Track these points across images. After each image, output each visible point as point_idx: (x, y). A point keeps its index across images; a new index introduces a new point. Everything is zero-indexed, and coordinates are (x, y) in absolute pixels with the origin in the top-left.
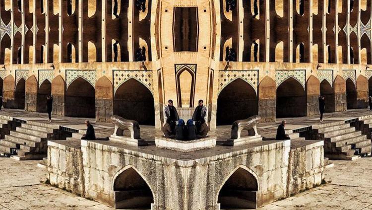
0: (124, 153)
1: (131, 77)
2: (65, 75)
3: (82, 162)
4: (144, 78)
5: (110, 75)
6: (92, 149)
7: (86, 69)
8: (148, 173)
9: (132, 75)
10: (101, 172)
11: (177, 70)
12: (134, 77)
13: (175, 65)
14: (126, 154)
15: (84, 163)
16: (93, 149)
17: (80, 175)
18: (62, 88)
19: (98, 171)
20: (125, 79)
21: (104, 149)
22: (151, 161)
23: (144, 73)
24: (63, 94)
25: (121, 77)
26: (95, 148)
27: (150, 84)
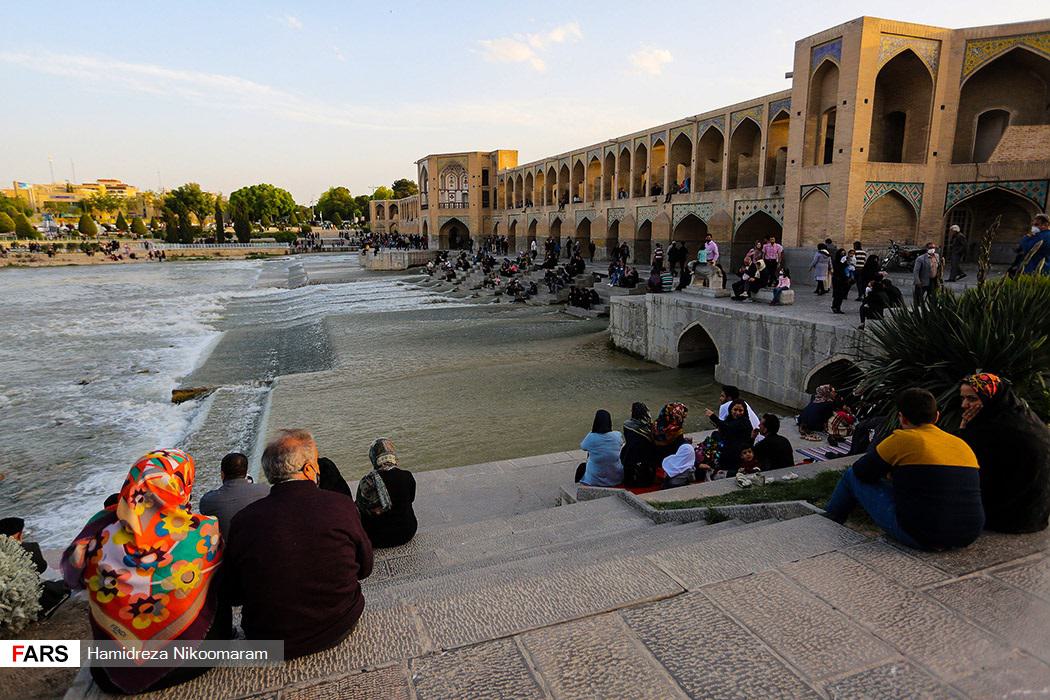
1: (758, 210)
5: (730, 210)
9: (761, 206)
13: (802, 187)
15: (649, 322)
24: (668, 238)
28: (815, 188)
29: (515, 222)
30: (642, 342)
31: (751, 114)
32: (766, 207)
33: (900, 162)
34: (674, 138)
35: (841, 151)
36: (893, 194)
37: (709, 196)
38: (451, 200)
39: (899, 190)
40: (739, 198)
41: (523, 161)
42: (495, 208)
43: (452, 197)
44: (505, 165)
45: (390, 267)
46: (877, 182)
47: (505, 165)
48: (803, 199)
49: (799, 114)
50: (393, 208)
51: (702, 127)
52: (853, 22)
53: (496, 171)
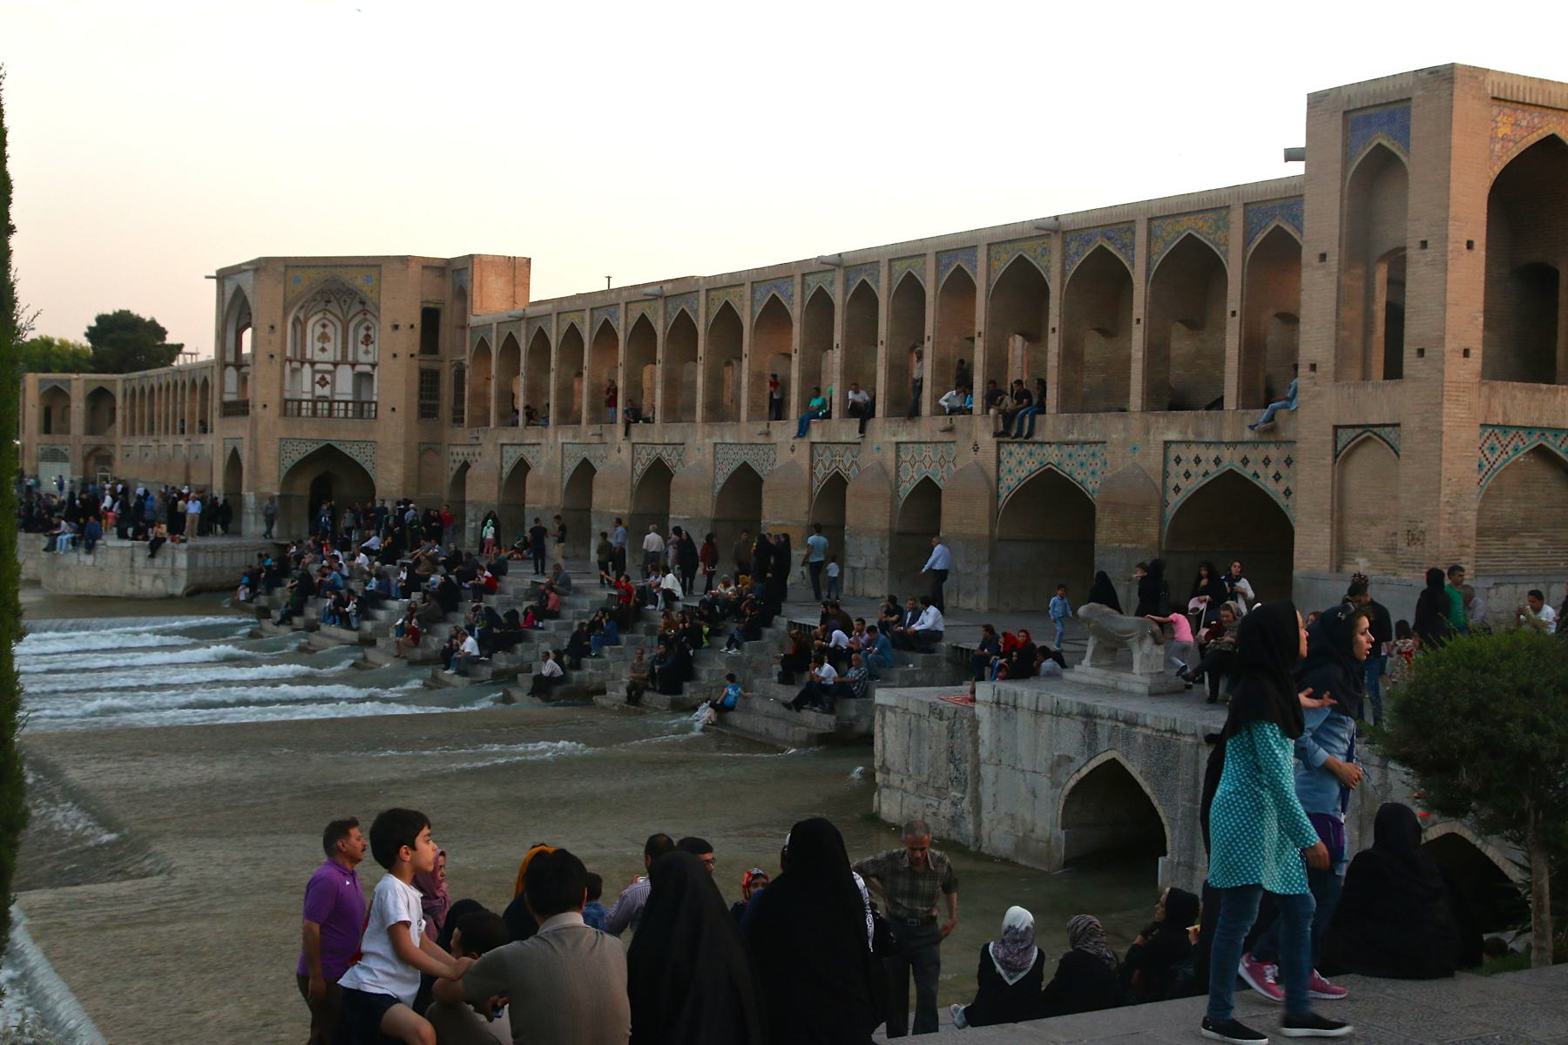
0: (1095, 717)
1: (1226, 466)
2: (993, 462)
3: (976, 751)
4: (1271, 471)
5: (1154, 461)
6: (1006, 710)
7: (1070, 437)
8: (1158, 773)
9: (1231, 460)
10: (1028, 776)
11: (1339, 448)
12: (1238, 467)
13: (1336, 428)
14: (1101, 717)
15: (984, 752)
16: (1010, 710)
17: (969, 790)
18: (981, 510)
19: (1021, 776)
20: (1206, 474)
21: (1040, 709)
22: (1168, 735)
23: (1273, 452)
24: (986, 532)
25: (1193, 469)
26: (1015, 707)
27: (1288, 493)
28: (1367, 434)
29: (522, 468)
30: (966, 804)
31: (1202, 229)
32: (1245, 461)
33: (1550, 380)
34: (1001, 267)
35: (1421, 352)
36: (1541, 452)
37: (1092, 426)
38: (319, 391)
39: (1551, 443)
40: (1172, 436)
41: (545, 287)
42: (458, 419)
43: (323, 382)
44: (490, 303)
45: (128, 589)
46: (1505, 428)
47: (490, 303)
48: (1341, 457)
49: (1323, 257)
50: (99, 398)
51: (1074, 246)
52: (1434, 72)
53: (464, 313)
